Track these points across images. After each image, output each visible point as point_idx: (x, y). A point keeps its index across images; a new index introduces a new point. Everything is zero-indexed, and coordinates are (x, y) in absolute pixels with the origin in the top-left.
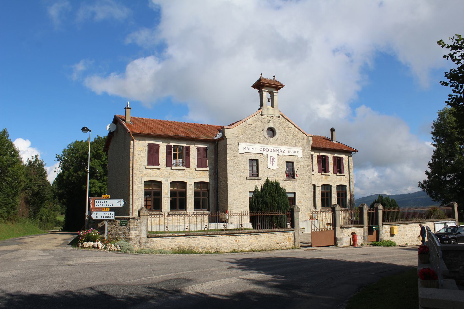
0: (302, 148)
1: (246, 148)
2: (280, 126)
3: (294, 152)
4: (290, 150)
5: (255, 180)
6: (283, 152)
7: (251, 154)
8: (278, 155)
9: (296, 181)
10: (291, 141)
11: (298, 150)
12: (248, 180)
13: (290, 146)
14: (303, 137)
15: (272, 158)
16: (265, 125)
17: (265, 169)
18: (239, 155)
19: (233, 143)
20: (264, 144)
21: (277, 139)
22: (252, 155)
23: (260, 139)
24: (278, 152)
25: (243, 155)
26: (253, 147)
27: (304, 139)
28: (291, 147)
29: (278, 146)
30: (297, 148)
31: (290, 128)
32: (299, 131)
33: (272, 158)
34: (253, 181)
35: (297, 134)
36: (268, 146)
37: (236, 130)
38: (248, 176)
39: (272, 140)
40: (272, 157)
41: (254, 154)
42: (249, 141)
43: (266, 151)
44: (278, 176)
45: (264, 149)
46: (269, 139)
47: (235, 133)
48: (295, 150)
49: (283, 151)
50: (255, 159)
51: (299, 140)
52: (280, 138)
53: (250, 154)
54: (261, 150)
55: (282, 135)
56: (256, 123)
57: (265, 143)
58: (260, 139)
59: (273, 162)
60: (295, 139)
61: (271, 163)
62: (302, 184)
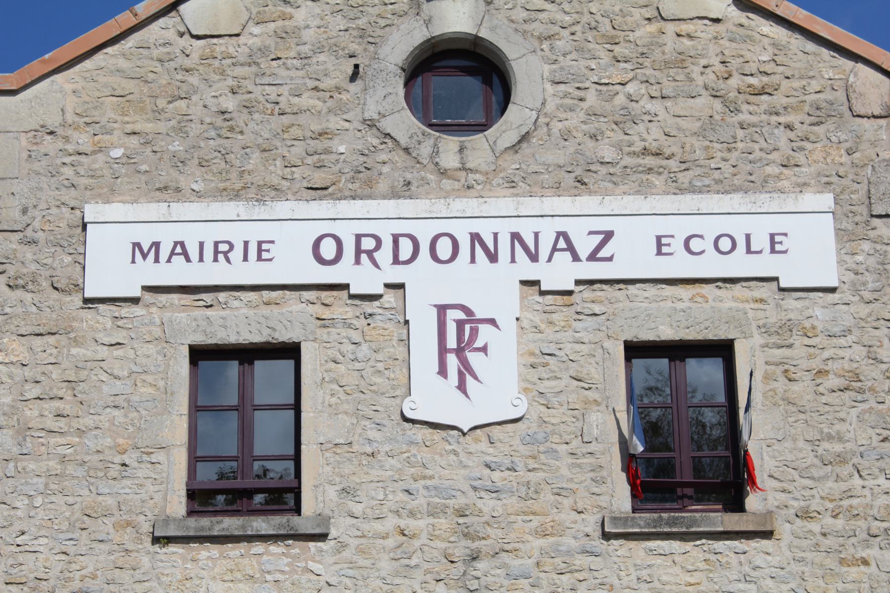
0: (827, 200)
1: (156, 245)
2: (559, 16)
3: (725, 244)
4: (680, 228)
5: (258, 548)
6: (593, 257)
7: (222, 296)
8: (524, 283)
9: (767, 535)
10: (693, 140)
11: (776, 224)
12: (173, 548)
13: (681, 191)
14: (841, 95)
15: (461, 315)
16: (383, 22)
17: (372, 434)
18: (88, 315)
19: (25, 211)
20: (370, 197)
21: (525, 138)
22: (236, 303)
23: (327, 151)
24: (534, 258)
25: (126, 310)
26: (237, 234)
27: (859, 109)
28: (688, 202)
29: (532, 205)
30: (765, 202)
31: (685, 28)
32: (797, 41)
33: (461, 315)
34: (234, 551)
35: (768, 68)
36: (406, 207)
37: (71, 104)
38: (178, 505)
39: (461, 150)
40: (454, 315)
41: (252, 296)
42: (195, 187)
43: (384, 255)
44: (531, 492)
45: (368, 244)
46: (425, 150)
47: (53, 121)
48: (738, 227)
49: (584, 247)
50: (257, 338)
51: (789, 127)
52: (556, 127)
53: (208, 297)
54: (328, 249)
55: (592, 98)
56: (284, 17)
57: (383, 186)
58: (327, 151)
59: (473, 358)
60: (742, 117)
61: (443, 371)
62: (842, 561)
